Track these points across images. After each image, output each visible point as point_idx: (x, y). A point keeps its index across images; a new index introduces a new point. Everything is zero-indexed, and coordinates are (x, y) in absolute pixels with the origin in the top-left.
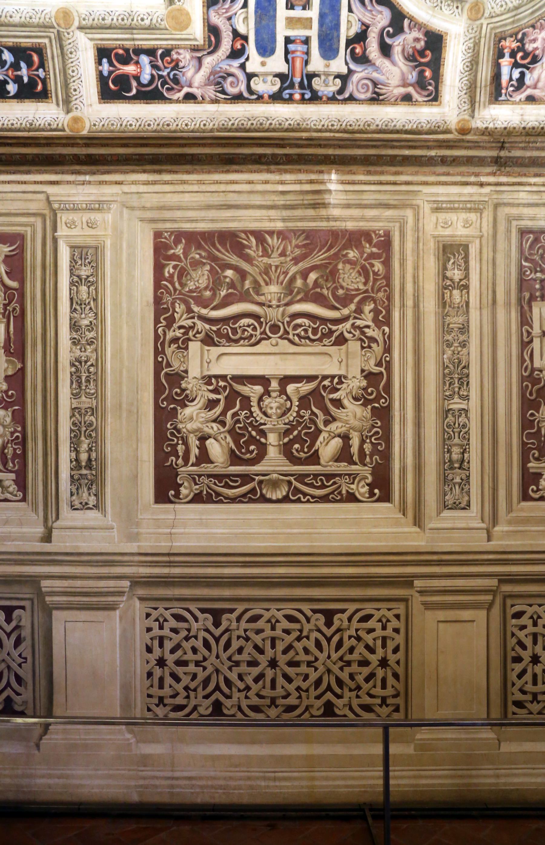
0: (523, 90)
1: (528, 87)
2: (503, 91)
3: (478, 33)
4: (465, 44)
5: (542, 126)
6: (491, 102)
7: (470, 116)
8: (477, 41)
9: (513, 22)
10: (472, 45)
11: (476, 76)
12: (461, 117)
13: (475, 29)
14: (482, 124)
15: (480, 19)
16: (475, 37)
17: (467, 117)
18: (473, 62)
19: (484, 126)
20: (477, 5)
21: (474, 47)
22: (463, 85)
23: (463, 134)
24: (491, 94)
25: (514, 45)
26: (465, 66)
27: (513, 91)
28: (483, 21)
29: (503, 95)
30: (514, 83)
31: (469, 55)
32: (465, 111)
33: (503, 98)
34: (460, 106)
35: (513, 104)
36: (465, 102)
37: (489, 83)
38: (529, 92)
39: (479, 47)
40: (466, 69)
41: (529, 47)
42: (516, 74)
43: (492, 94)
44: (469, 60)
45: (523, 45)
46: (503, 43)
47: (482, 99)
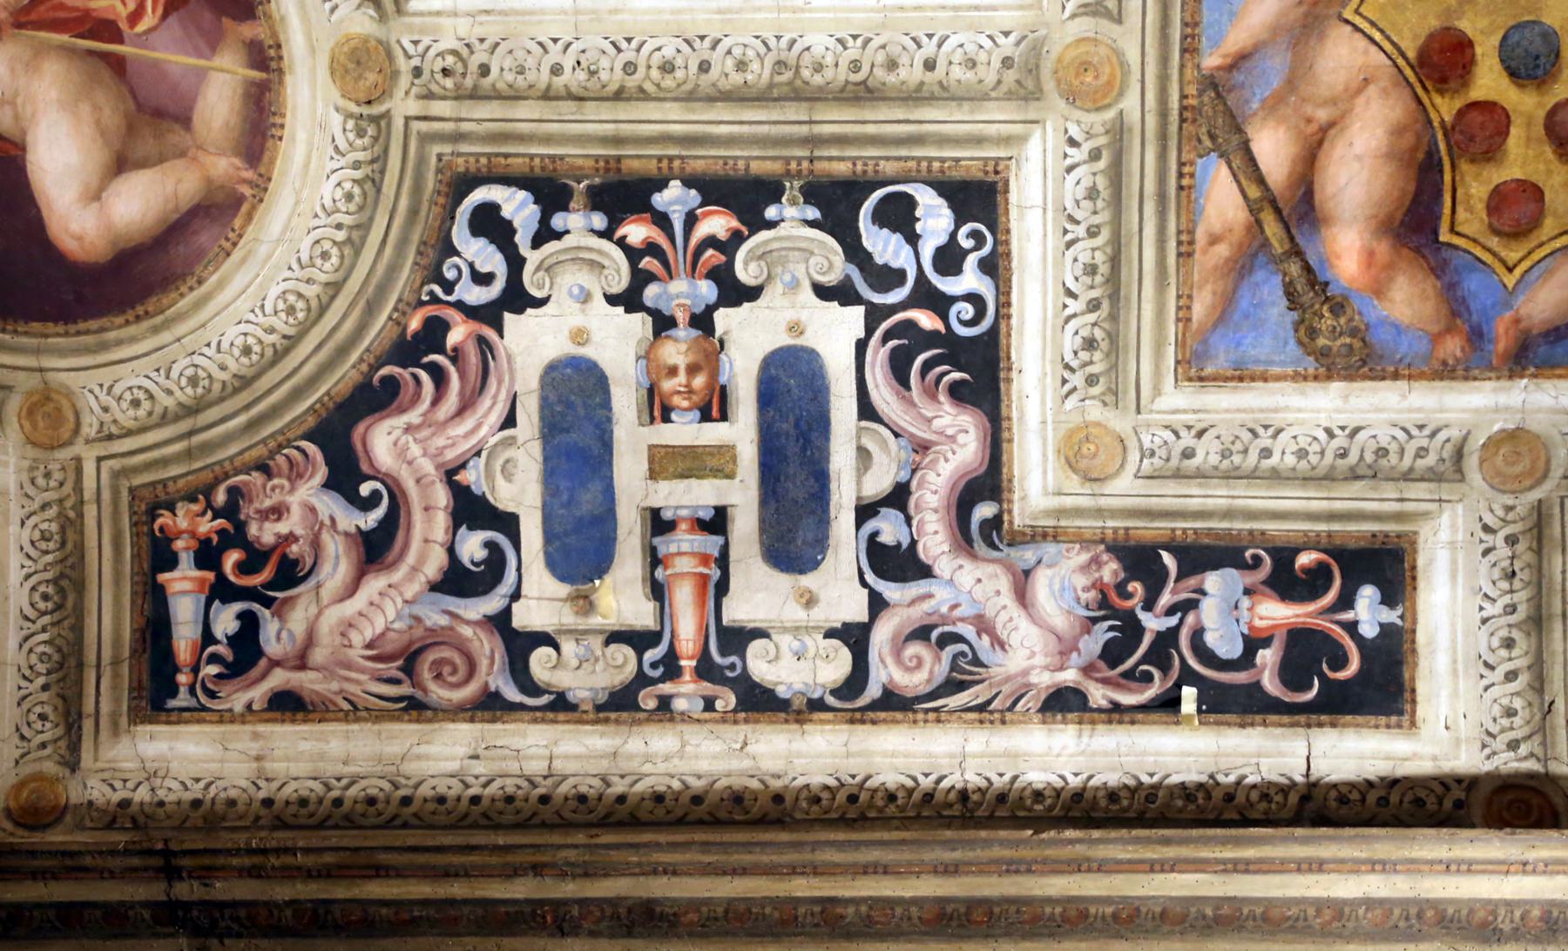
0: (255, 672)
1: (275, 663)
2: (182, 678)
3: (68, 488)
4: (30, 523)
5: (335, 794)
6: (137, 717)
7: (64, 763)
8: (72, 514)
9: (189, 454)
10: (54, 527)
11: (78, 628)
12: (27, 769)
13: (57, 476)
14: (107, 790)
15: (69, 443)
16: (61, 501)
17: (50, 767)
18: (65, 583)
19: (116, 797)
20: (48, 399)
21: (63, 530)
22: (34, 659)
23: (32, 828)
24: (136, 689)
25: (207, 526)
26: (37, 597)
27: (219, 676)
28: (78, 448)
29: (182, 689)
30: (222, 649)
31: (49, 558)
32: (43, 745)
33: (182, 699)
34: (26, 731)
35: (221, 721)
36: (43, 717)
37: (126, 653)
38: (278, 679)
39: (81, 533)
40: (42, 605)
41: (265, 533)
42: (226, 621)
43: (140, 687)
44: (49, 575)
45: (241, 527)
46: (165, 519)
47: (105, 708)
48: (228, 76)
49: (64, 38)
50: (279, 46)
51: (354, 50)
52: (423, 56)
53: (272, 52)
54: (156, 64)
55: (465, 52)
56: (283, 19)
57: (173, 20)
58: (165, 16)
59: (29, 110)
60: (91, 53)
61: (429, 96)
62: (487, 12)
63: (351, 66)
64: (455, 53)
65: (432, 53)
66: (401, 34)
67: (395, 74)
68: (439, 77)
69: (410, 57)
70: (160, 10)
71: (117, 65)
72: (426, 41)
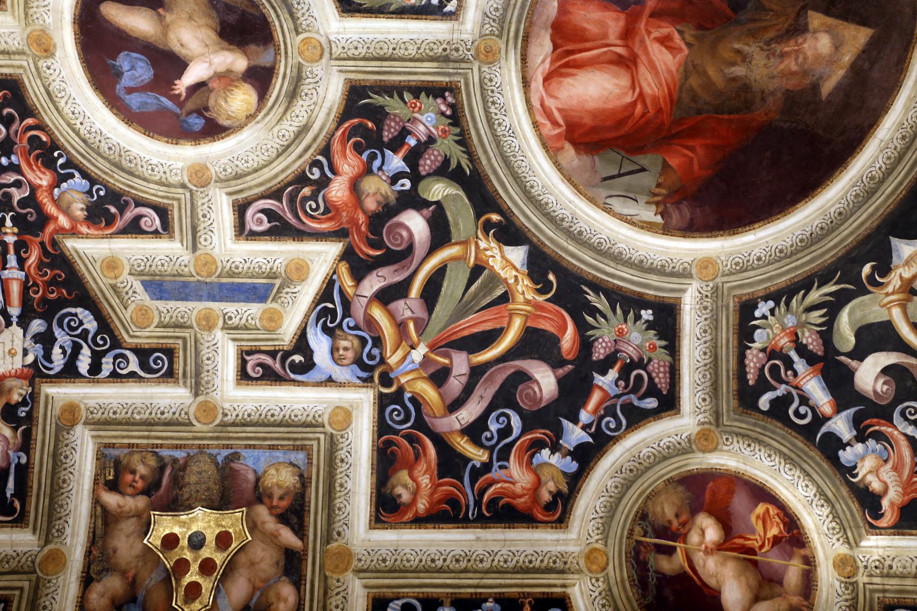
48: (796, 568)
49: (735, 554)
50: (814, 557)
51: (842, 559)
52: (867, 561)
53: (812, 559)
54: (769, 563)
55: (882, 560)
56: (815, 548)
57: (775, 548)
58: (772, 547)
59: (722, 579)
60: (745, 559)
61: (871, 576)
62: (889, 547)
63: (841, 564)
64: (878, 560)
65: (870, 560)
66: (859, 554)
67: (858, 568)
68: (874, 569)
69: (862, 562)
70: (770, 545)
71: (755, 563)
72: (868, 556)
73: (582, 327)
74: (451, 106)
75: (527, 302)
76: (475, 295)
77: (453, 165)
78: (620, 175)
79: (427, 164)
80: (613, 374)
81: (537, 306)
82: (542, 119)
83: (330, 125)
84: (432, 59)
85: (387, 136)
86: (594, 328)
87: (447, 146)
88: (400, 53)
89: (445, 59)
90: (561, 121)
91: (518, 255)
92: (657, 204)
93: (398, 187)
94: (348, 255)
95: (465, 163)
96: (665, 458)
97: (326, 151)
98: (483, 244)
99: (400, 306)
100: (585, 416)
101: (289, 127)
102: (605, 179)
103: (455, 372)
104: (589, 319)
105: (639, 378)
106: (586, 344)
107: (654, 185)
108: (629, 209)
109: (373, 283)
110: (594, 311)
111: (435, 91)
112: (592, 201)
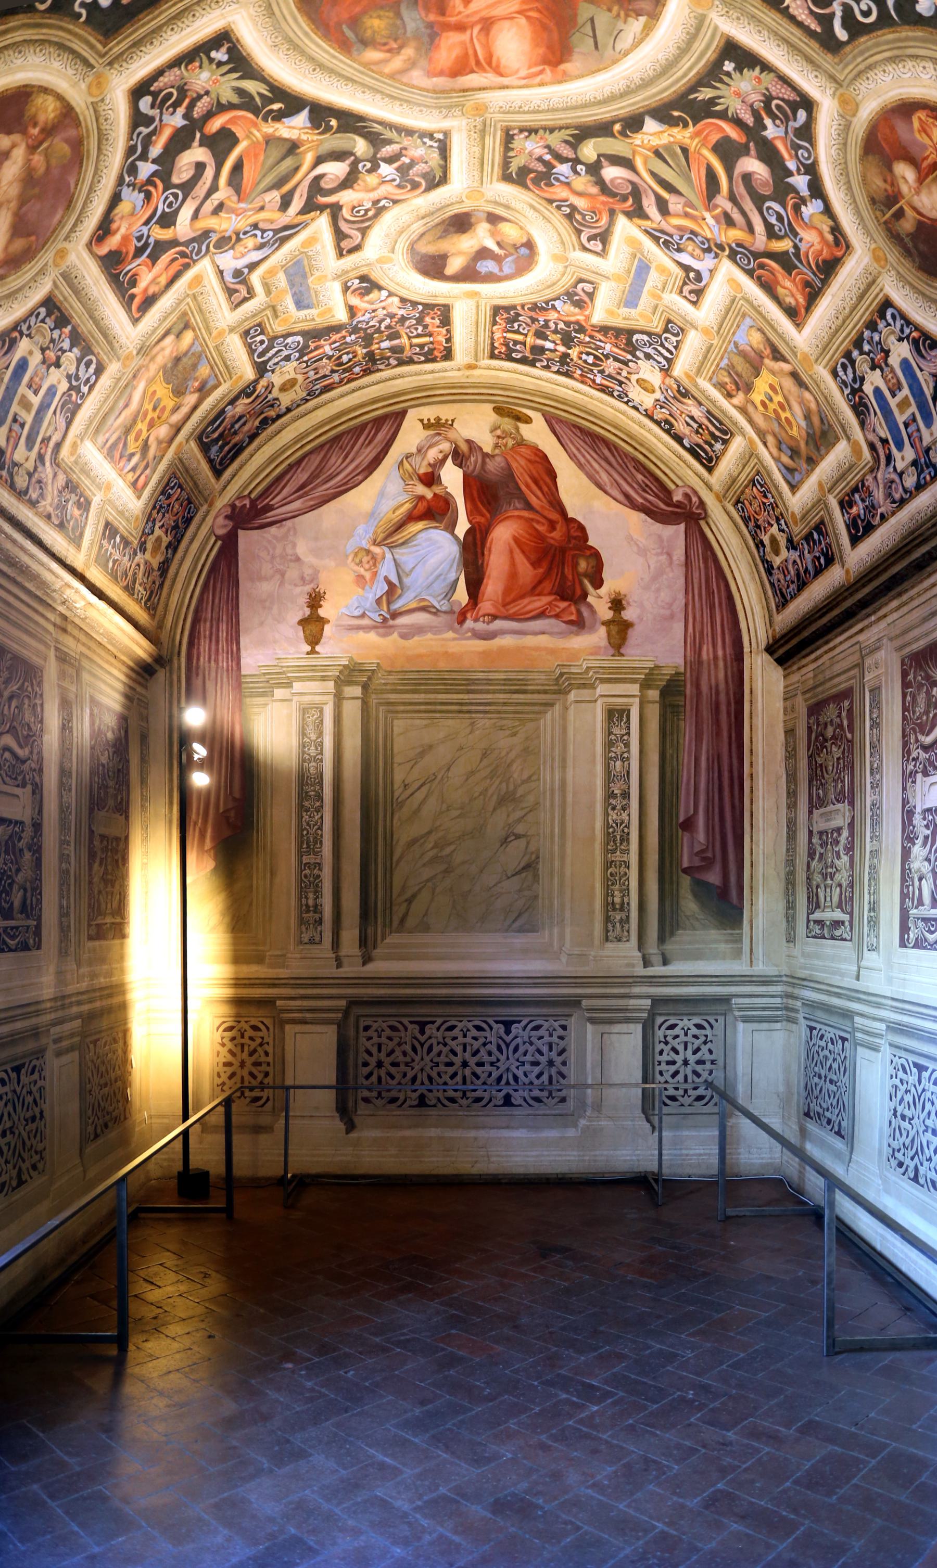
73: (723, 115)
74: (521, 131)
75: (692, 138)
76: (678, 165)
77: (570, 139)
78: (595, 36)
79: (567, 152)
80: (768, 122)
81: (697, 134)
82: (538, 79)
83: (530, 194)
84: (483, 138)
85: (541, 168)
86: (727, 109)
87: (555, 140)
88: (477, 155)
89: (483, 133)
90: (541, 68)
91: (651, 125)
92: (627, 16)
93: (583, 173)
94: (629, 215)
95: (569, 132)
96: (845, 144)
97: (550, 201)
98: (638, 142)
99: (672, 207)
100: (791, 165)
101: (530, 213)
102: (596, 47)
103: (729, 210)
104: (718, 108)
105: (778, 106)
106: (738, 122)
107: (608, 14)
108: (626, 41)
109: (652, 210)
110: (712, 102)
111: (508, 138)
112: (615, 62)
